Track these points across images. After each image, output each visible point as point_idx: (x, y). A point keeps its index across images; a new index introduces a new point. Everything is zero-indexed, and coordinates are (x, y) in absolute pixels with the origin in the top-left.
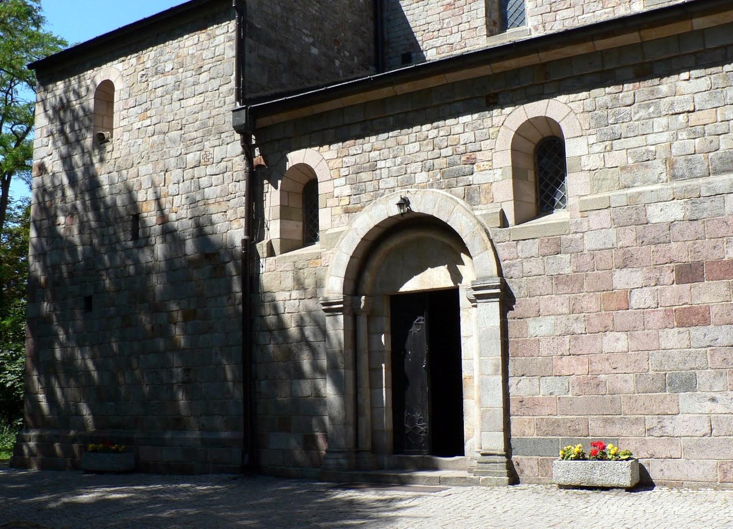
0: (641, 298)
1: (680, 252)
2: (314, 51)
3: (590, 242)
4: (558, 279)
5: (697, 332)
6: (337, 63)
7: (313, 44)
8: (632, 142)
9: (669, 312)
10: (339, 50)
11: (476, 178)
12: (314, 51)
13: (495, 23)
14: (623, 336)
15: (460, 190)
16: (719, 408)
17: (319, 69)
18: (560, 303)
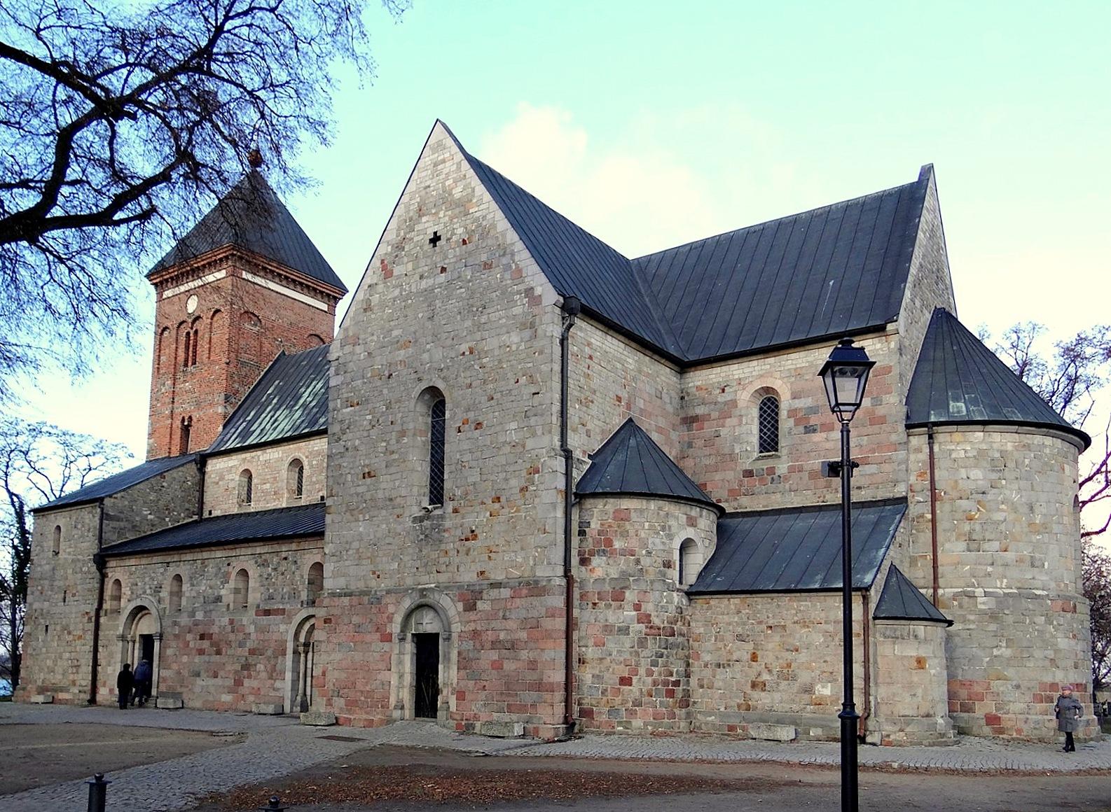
0: (192, 645)
1: (201, 629)
2: (150, 517)
3: (182, 625)
4: (175, 635)
5: (202, 657)
6: (167, 519)
7: (150, 514)
8: (197, 588)
9: (197, 650)
10: (169, 513)
11: (161, 594)
12: (150, 517)
13: (243, 501)
14: (186, 657)
15: (157, 597)
16: (204, 683)
17: (153, 526)
18: (174, 644)
